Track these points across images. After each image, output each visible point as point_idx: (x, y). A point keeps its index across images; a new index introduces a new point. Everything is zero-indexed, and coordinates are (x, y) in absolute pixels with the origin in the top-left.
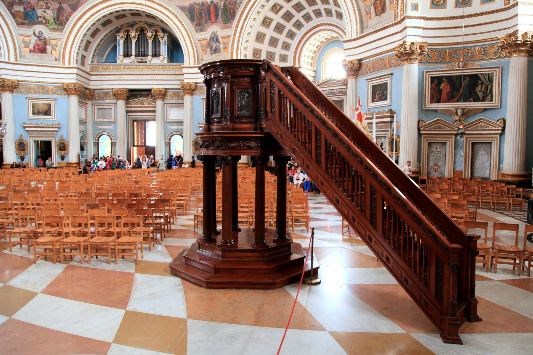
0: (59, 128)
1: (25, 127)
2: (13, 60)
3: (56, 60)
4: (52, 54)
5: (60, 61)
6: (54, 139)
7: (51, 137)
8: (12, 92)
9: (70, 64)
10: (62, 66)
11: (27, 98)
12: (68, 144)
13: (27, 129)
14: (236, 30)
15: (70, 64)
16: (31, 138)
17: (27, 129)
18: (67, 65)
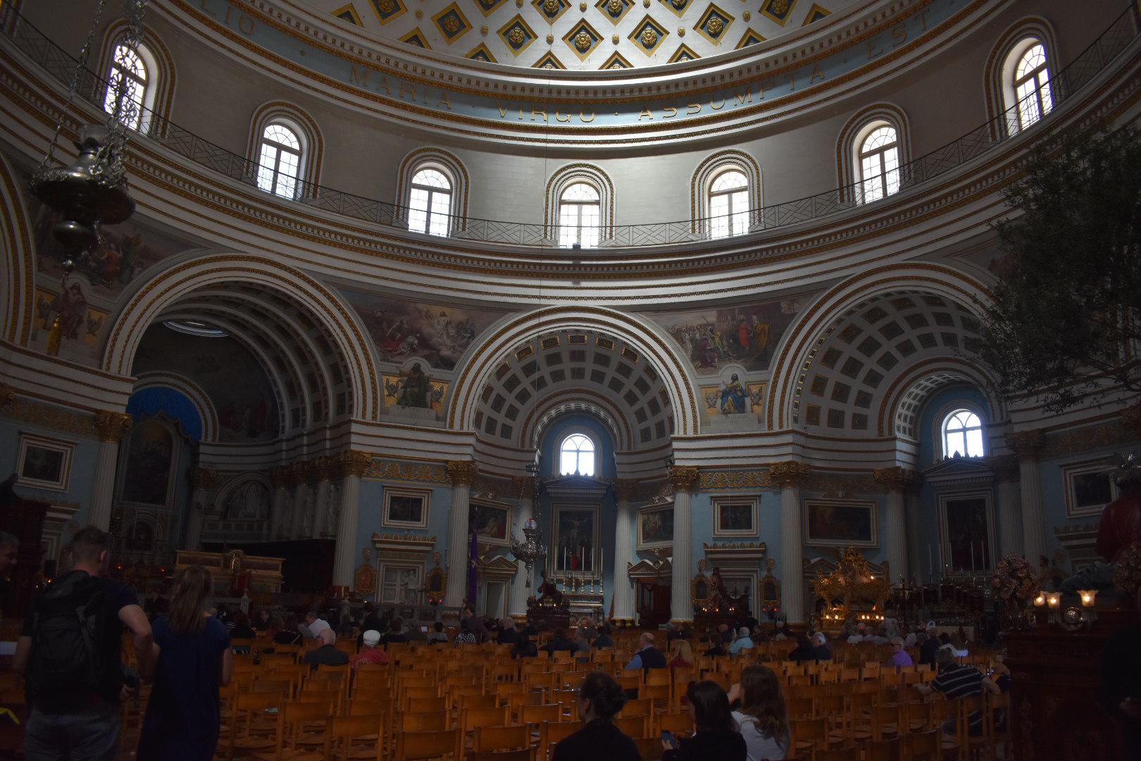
0: (432, 545)
1: (375, 542)
3: (438, 419)
4: (431, 408)
5: (446, 421)
7: (418, 563)
8: (360, 475)
9: (462, 427)
10: (448, 429)
11: (383, 487)
12: (447, 578)
13: (378, 545)
14: (778, 372)
16: (382, 564)
17: (378, 545)
18: (457, 428)
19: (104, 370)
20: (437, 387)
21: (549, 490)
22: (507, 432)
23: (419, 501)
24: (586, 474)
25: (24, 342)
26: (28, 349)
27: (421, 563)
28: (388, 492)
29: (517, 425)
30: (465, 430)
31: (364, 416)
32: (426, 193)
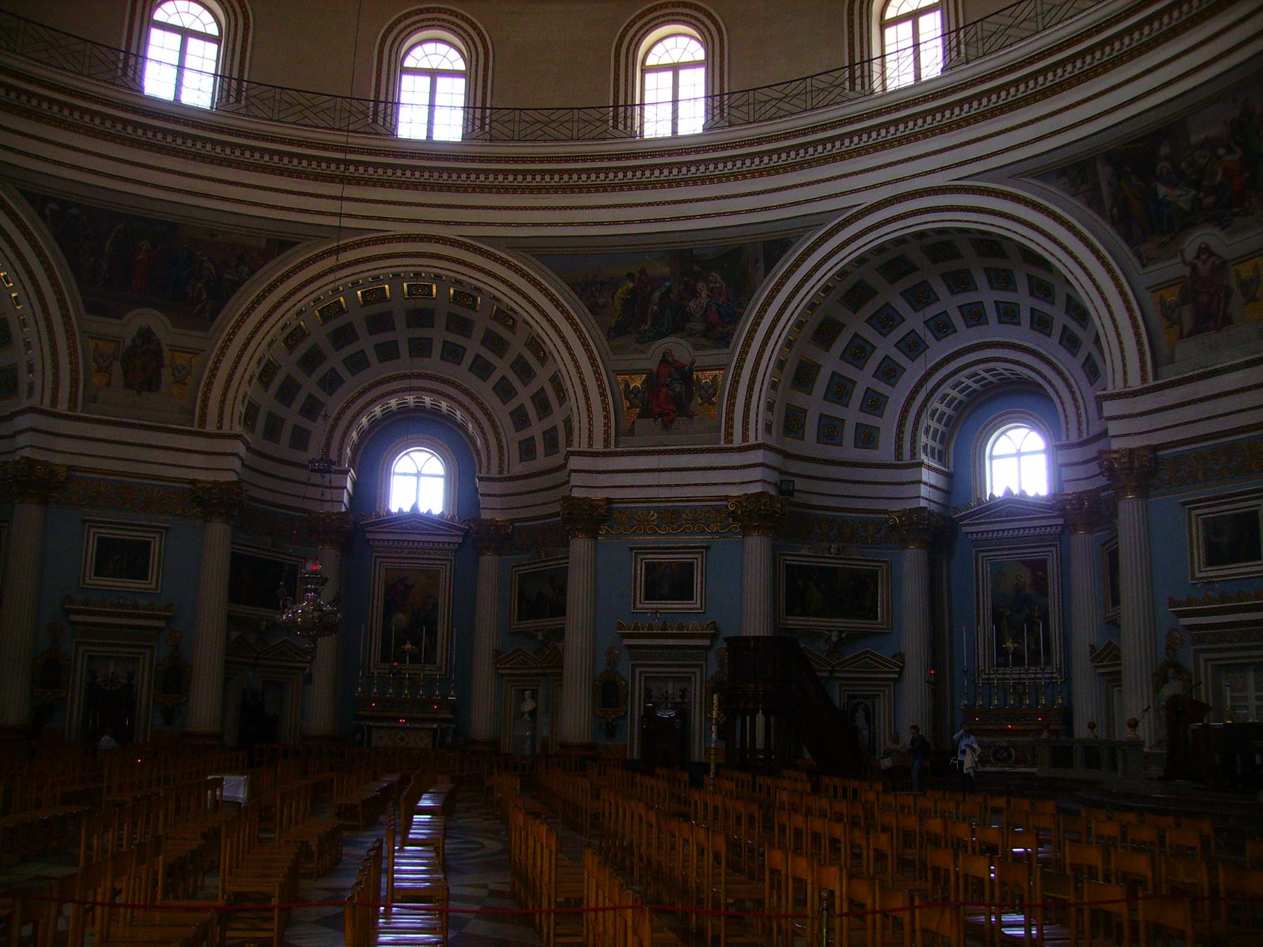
2: (598, 446)
6: (697, 670)
7: (691, 666)
8: (593, 533)
9: (745, 437)
10: (722, 444)
11: (631, 549)
15: (745, 437)
19: (195, 428)
20: (706, 377)
21: (966, 529)
22: (867, 437)
23: (688, 569)
24: (1008, 492)
25: (72, 406)
26: (79, 413)
27: (696, 666)
28: (640, 557)
29: (887, 425)
30: (752, 441)
31: (590, 445)
32: (669, 75)
